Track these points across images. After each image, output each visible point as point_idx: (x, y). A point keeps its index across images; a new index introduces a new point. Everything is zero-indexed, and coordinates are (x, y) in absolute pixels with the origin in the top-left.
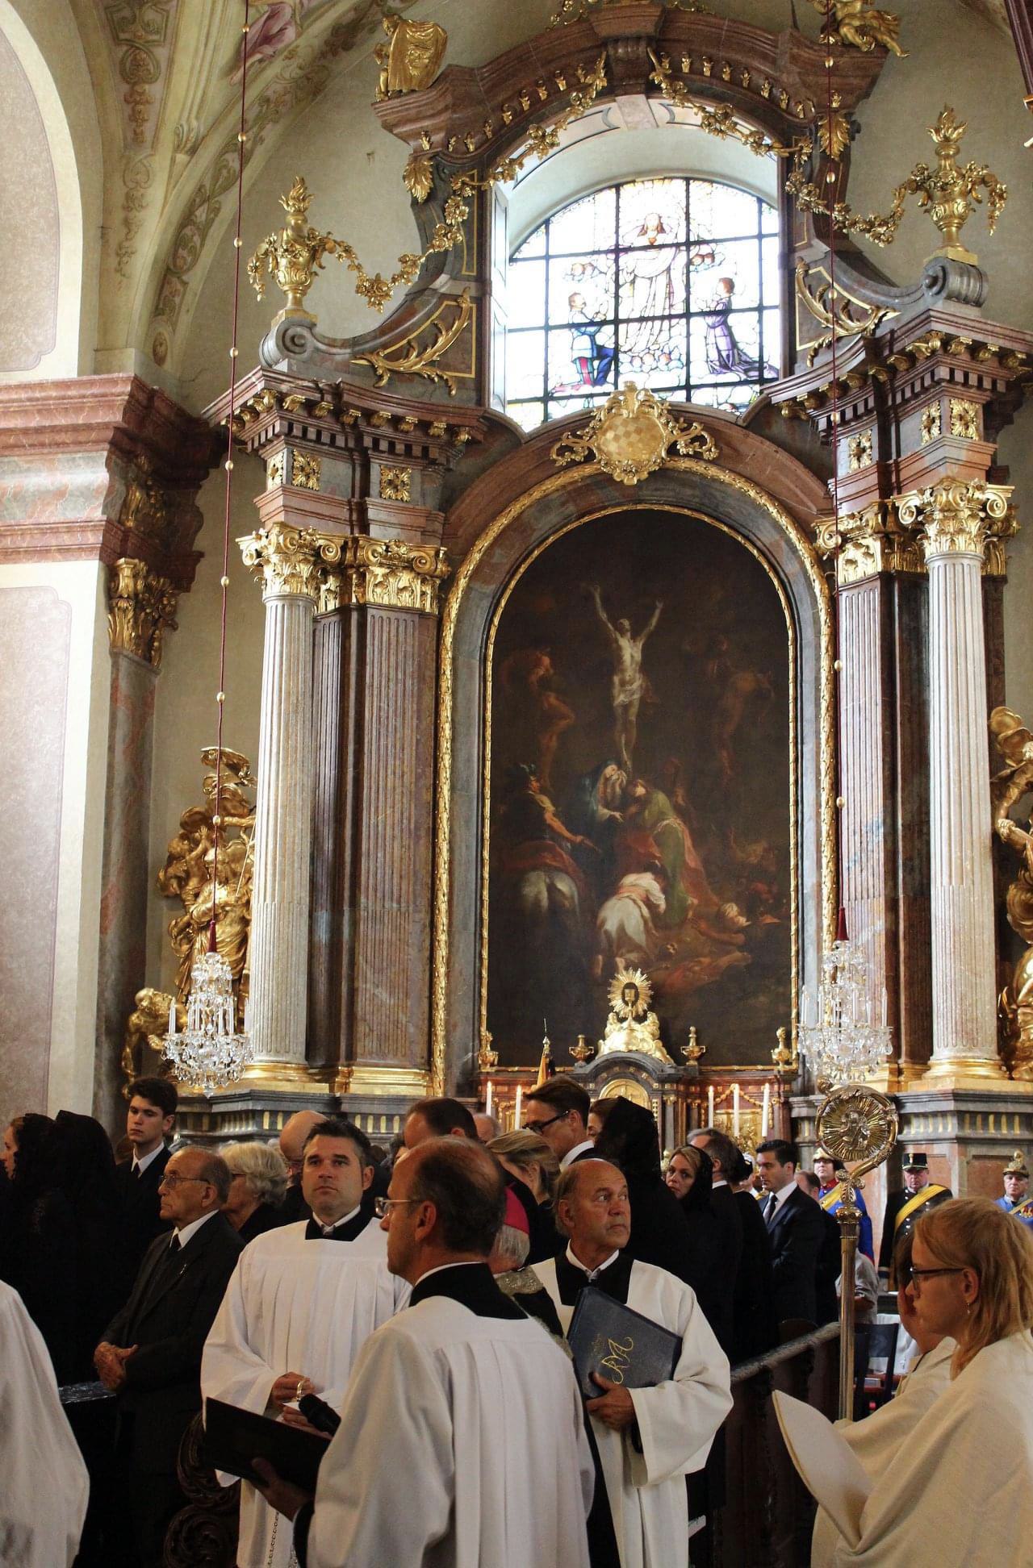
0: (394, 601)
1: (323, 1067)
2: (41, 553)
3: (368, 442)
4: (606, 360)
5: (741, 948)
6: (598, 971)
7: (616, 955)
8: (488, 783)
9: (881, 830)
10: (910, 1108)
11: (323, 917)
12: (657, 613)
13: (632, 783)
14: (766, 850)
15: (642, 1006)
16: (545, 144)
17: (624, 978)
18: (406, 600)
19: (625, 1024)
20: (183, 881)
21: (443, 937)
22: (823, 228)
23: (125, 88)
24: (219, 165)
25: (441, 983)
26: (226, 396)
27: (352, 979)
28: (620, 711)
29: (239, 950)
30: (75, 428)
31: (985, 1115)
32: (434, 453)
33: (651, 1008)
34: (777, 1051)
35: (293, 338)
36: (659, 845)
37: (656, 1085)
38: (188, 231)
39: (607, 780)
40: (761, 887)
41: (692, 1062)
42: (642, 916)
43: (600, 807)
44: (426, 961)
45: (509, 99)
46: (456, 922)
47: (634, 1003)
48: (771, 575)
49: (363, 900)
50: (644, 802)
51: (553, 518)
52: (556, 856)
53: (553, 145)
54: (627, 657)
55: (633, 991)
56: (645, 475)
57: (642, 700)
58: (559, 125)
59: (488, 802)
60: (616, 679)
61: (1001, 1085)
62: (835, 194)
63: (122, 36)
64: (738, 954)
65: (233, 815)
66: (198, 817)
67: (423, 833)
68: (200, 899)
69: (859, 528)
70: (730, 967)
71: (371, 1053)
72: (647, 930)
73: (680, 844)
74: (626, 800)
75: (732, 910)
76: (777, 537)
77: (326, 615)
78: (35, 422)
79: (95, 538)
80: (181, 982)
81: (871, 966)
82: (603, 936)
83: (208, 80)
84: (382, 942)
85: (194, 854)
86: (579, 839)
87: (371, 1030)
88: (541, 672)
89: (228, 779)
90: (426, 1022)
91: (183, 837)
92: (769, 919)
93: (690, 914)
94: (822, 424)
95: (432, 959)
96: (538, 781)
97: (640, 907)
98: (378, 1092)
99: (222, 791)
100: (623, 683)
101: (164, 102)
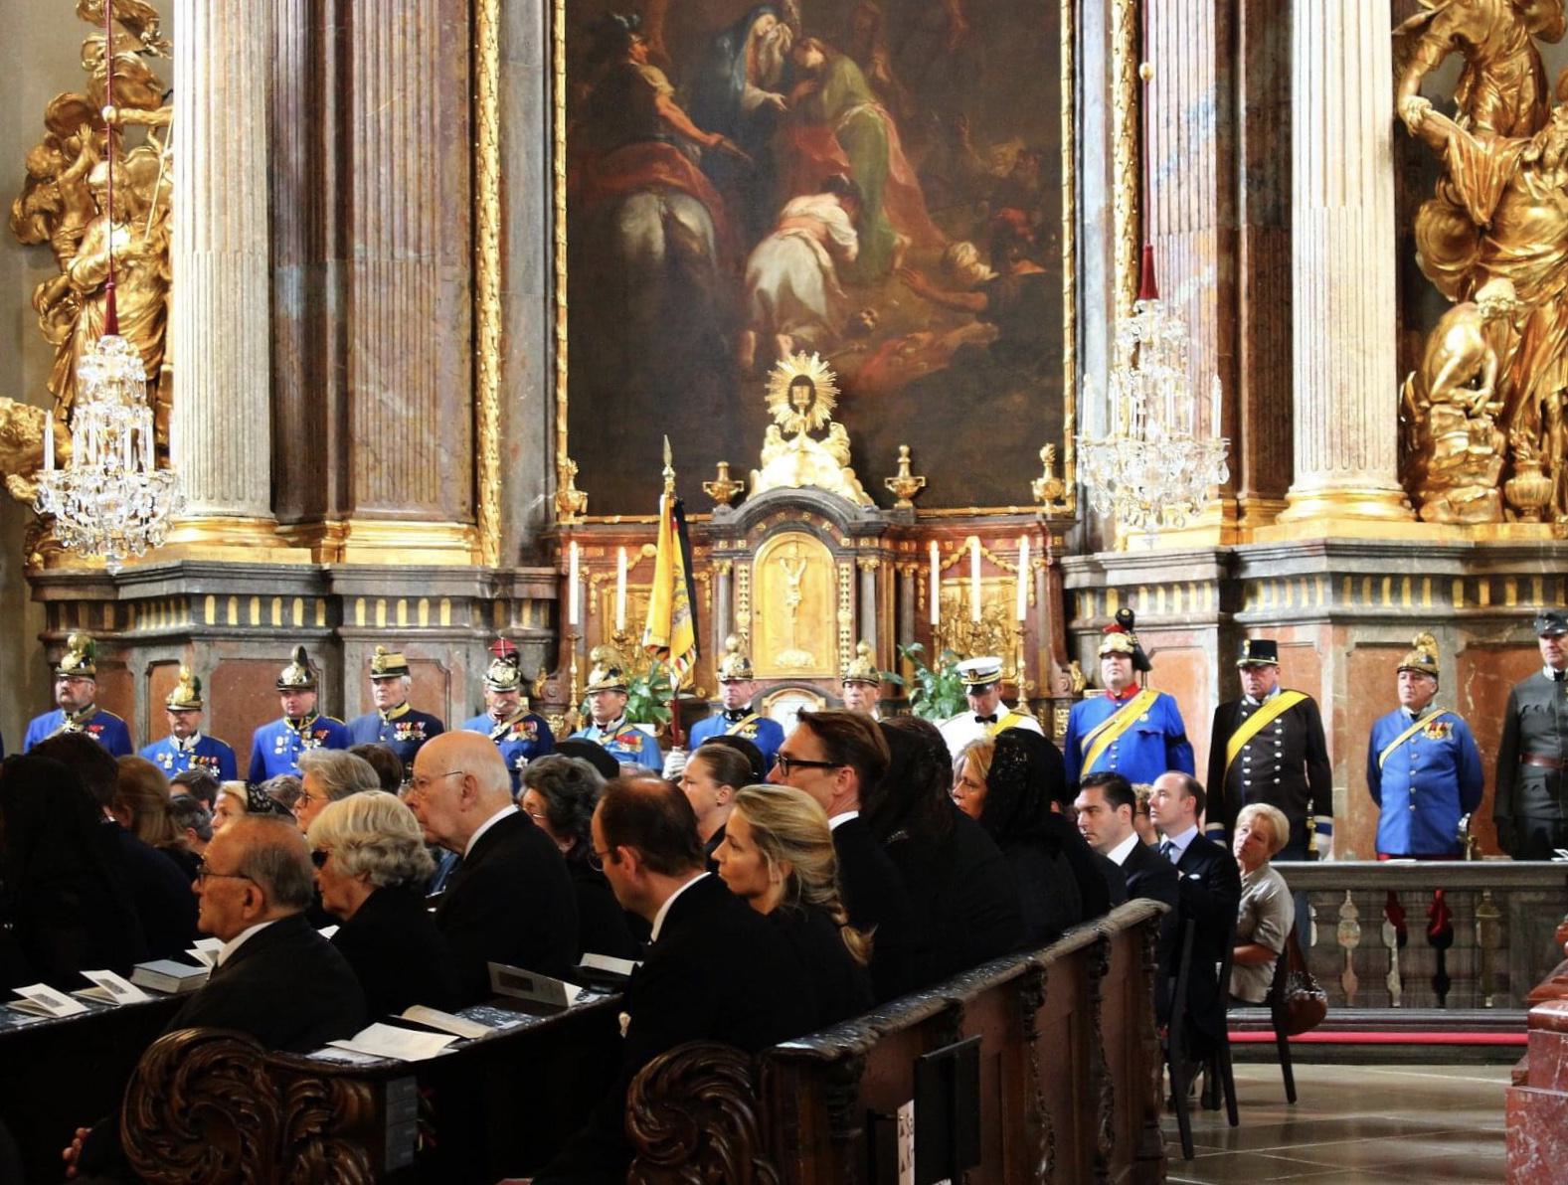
1: (301, 522)
5: (982, 316)
7: (779, 331)
8: (561, 47)
9: (1212, 118)
10: (1255, 570)
11: (293, 276)
13: (800, 44)
14: (1021, 153)
15: (822, 412)
17: (790, 367)
19: (794, 443)
20: (53, 218)
21: (491, 306)
25: (491, 380)
27: (344, 377)
31: (1377, 579)
33: (837, 415)
34: (1041, 482)
36: (845, 148)
37: (845, 542)
39: (759, 39)
40: (1015, 215)
41: (904, 504)
42: (820, 266)
43: (748, 86)
44: (466, 346)
46: (513, 281)
47: (808, 409)
49: (358, 245)
50: (820, 77)
52: (676, 168)
55: (806, 390)
59: (561, 80)
61: (1402, 529)
64: (976, 326)
65: (134, 106)
66: (75, 109)
67: (454, 131)
68: (85, 247)
70: (964, 347)
71: (378, 499)
73: (879, 147)
74: (791, 74)
75: (967, 254)
80: (58, 387)
81: (1195, 341)
82: (755, 301)
84: (391, 315)
85: (71, 172)
86: (713, 139)
87: (378, 460)
89: (123, 42)
90: (468, 445)
91: (51, 144)
92: (1028, 268)
93: (899, 262)
95: (474, 341)
96: (644, 42)
97: (815, 251)
98: (392, 559)
99: (114, 63)
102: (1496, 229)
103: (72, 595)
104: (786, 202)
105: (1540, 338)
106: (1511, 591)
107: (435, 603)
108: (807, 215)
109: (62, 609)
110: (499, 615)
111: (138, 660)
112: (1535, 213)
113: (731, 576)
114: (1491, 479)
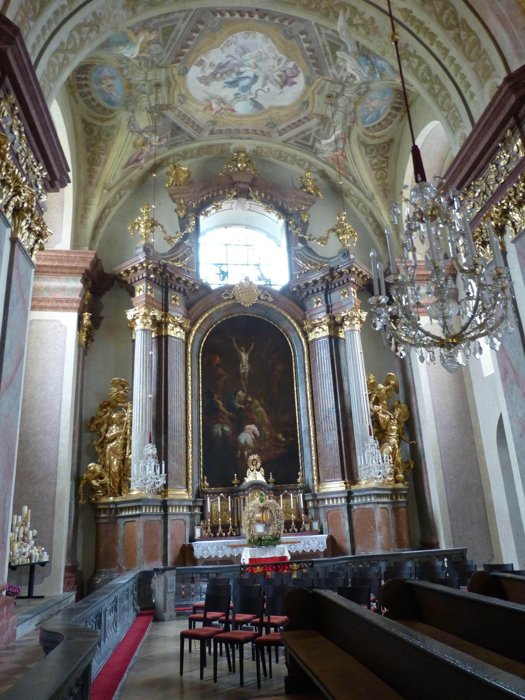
0: (176, 336)
2: (56, 309)
3: (169, 285)
4: (224, 274)
6: (239, 456)
10: (355, 494)
12: (252, 346)
13: (247, 397)
16: (217, 207)
18: (179, 335)
19: (254, 472)
20: (99, 426)
22: (302, 240)
23: (88, 166)
24: (114, 198)
26: (128, 263)
29: (123, 450)
30: (70, 268)
32: (187, 292)
33: (261, 466)
35: (148, 249)
37: (267, 491)
38: (103, 215)
39: (239, 396)
45: (205, 194)
47: (256, 465)
48: (286, 337)
50: (251, 403)
51: (220, 316)
53: (220, 208)
56: (251, 305)
57: (249, 372)
58: (222, 203)
60: (241, 365)
62: (304, 231)
63: (91, 149)
64: (282, 450)
65: (121, 403)
69: (320, 323)
74: (245, 402)
75: (280, 436)
77: (152, 338)
78: (56, 264)
79: (76, 305)
80: (101, 461)
83: (117, 168)
86: (231, 414)
88: (217, 362)
92: (291, 439)
93: (267, 437)
94: (305, 294)
95: (187, 452)
96: (217, 395)
100: (243, 366)
101: (101, 173)
102: (386, 430)
103: (105, 507)
105: (396, 451)
106: (399, 497)
107: (183, 507)
109: (102, 510)
110: (192, 509)
111: (121, 522)
112: (393, 427)
113: (244, 499)
114: (393, 476)
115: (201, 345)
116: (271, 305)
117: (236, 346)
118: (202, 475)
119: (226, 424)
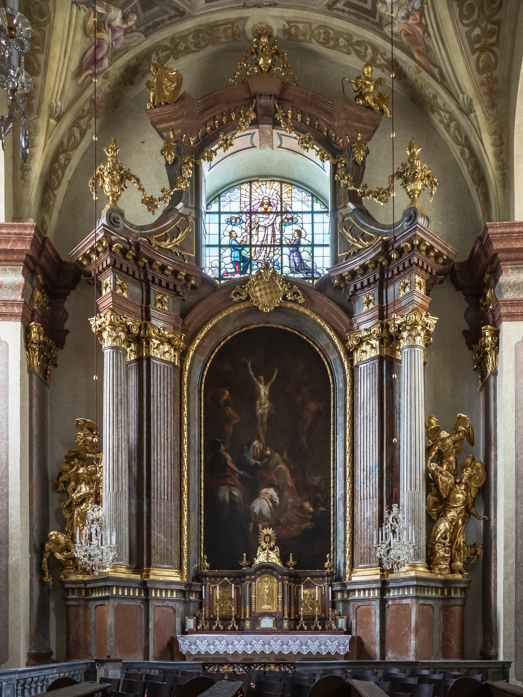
6: (251, 529)
7: (259, 523)
12: (275, 374)
13: (265, 449)
28: (259, 417)
36: (276, 476)
39: (254, 447)
42: (269, 506)
50: (270, 457)
51: (230, 327)
54: (262, 393)
57: (269, 412)
60: (258, 403)
72: (271, 513)
74: (262, 456)
76: (328, 341)
86: (242, 472)
88: (225, 398)
96: (224, 446)
97: (268, 503)
100: (261, 405)
104: (260, 490)
108: (267, 493)
115: (203, 373)
116: (302, 309)
117: (252, 374)
118: (202, 554)
119: (236, 486)
